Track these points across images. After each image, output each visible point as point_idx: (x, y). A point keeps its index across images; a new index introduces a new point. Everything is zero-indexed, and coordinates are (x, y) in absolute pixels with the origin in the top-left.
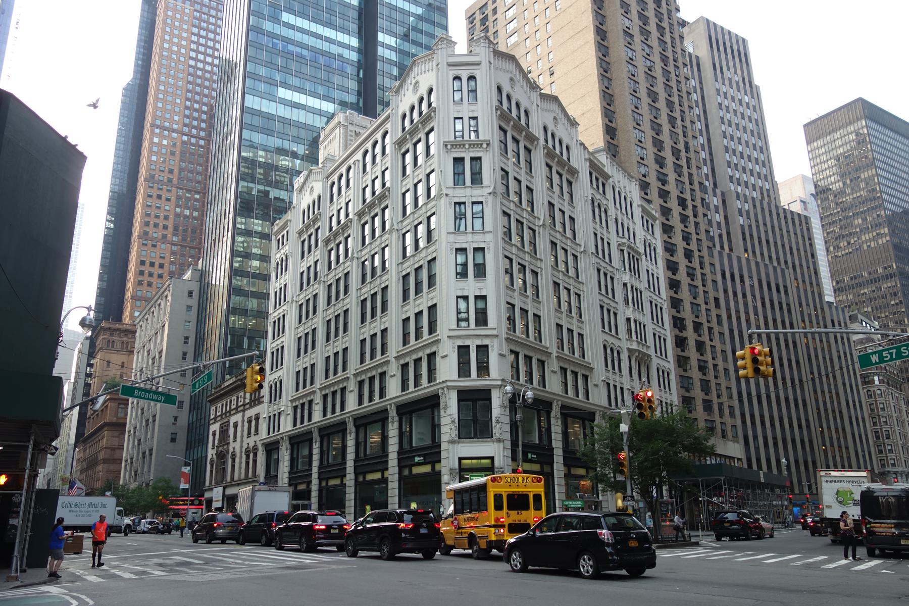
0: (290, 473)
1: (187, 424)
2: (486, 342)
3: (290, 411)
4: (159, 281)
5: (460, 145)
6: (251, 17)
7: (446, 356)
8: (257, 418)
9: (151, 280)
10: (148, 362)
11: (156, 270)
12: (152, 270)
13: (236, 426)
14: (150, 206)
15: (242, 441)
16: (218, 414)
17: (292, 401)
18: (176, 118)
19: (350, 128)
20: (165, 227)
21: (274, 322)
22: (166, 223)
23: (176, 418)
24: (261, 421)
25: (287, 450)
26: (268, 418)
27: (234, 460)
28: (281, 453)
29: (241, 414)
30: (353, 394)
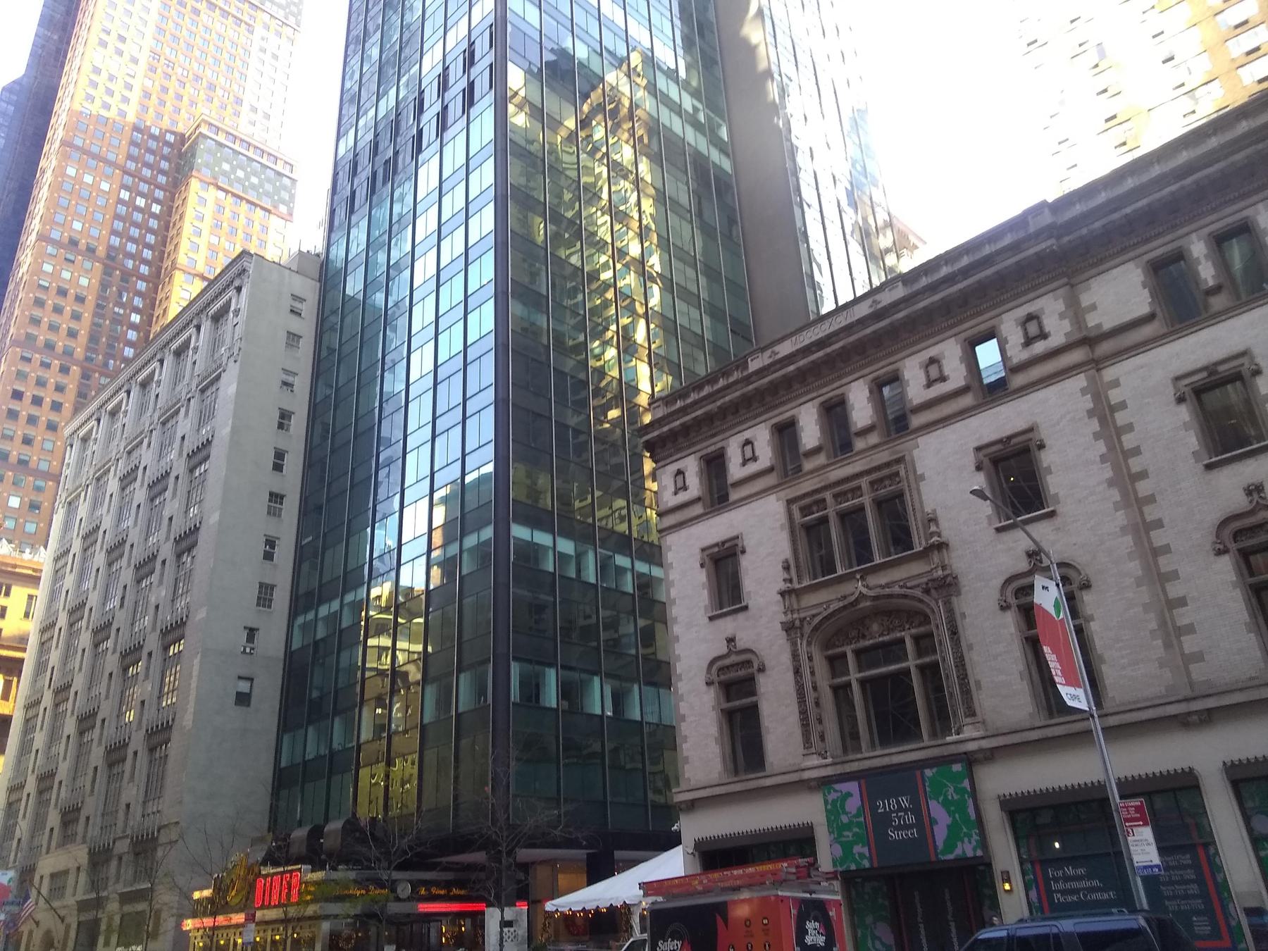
1: (281, 654)
4: (49, 435)
9: (31, 431)
11: (45, 414)
12: (34, 411)
20: (72, 334)
22: (74, 325)
23: (252, 633)
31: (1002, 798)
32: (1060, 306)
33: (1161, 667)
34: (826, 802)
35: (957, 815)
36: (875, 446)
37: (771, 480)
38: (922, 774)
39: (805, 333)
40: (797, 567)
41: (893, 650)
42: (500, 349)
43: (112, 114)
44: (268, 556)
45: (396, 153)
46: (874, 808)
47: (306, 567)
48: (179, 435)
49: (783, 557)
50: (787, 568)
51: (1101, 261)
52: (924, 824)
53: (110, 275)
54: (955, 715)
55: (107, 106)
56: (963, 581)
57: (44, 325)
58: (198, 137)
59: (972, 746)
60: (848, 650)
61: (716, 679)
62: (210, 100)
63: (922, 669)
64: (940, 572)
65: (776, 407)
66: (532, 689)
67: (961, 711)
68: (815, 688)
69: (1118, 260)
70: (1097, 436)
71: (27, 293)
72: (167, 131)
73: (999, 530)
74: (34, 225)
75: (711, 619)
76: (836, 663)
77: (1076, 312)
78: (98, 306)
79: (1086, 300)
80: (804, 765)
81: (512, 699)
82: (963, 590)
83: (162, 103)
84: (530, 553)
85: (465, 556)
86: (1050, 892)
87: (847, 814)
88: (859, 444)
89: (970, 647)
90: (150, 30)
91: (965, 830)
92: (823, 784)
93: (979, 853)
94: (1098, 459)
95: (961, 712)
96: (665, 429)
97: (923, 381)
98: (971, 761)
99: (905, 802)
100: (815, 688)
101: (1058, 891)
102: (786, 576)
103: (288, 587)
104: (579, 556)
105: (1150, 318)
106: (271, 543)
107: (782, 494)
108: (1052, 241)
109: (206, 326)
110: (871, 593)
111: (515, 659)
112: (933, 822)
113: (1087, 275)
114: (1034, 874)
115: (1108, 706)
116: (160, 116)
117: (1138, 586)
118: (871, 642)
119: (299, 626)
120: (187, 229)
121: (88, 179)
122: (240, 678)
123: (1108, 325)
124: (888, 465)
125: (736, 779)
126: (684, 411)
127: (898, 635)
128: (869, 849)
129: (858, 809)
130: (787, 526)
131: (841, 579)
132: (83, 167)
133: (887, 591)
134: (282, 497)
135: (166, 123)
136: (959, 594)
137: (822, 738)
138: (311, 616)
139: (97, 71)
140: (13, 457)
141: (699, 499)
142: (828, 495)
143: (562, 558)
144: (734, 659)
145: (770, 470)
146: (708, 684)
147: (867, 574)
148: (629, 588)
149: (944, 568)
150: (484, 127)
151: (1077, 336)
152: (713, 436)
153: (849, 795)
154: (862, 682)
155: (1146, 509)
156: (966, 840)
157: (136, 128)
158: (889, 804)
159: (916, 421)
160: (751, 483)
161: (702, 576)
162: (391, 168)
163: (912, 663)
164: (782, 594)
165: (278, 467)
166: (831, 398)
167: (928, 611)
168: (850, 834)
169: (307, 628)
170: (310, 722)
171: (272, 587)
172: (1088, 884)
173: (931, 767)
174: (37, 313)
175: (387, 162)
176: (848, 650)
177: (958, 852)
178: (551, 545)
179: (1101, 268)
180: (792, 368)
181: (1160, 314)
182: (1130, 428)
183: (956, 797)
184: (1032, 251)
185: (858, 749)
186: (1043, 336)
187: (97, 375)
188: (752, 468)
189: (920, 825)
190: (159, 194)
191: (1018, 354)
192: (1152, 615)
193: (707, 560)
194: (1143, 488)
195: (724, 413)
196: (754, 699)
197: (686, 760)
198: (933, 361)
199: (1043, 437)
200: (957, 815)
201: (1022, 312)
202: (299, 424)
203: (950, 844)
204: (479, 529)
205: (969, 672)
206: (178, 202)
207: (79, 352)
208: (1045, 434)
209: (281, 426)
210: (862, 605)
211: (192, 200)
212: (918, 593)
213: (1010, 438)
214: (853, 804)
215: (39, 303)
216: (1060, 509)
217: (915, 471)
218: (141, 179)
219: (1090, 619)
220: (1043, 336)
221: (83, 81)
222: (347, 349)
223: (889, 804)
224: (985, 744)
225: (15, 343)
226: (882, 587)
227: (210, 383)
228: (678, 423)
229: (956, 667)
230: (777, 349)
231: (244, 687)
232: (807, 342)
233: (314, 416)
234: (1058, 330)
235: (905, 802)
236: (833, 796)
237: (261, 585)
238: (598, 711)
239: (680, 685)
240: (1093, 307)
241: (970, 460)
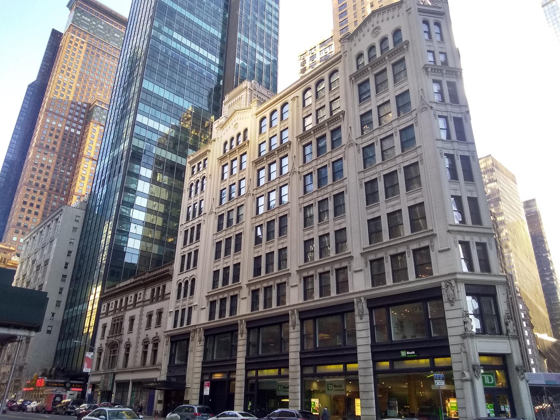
0: (203, 363)
2: (484, 240)
3: (205, 304)
4: (35, 217)
5: (438, 70)
6: (153, 30)
7: (448, 250)
8: (160, 313)
9: (29, 216)
10: (32, 270)
11: (34, 209)
12: (30, 208)
13: (132, 320)
14: (37, 164)
15: (139, 333)
16: (110, 309)
17: (208, 297)
18: (64, 109)
19: (254, 92)
20: (45, 180)
21: (186, 232)
23: (53, 314)
24: (163, 315)
25: (200, 341)
26: (174, 312)
27: (128, 349)
28: (191, 344)
29: (140, 309)
30: (296, 289)
43: (64, 98)
44: (60, 293)
53: (60, 158)
55: (62, 95)
58: (94, 107)
59: (115, 371)
62: (101, 90)
71: (30, 166)
72: (84, 103)
74: (35, 140)
78: (55, 170)
83: (83, 92)
120: (88, 141)
121: (54, 123)
122: (49, 326)
132: (52, 119)
139: (59, 82)
140: (23, 224)
157: (73, 103)
165: (66, 267)
171: (61, 301)
174: (33, 173)
187: (53, 195)
190: (80, 127)
202: (74, 255)
206: (86, 130)
207: (47, 187)
209: (68, 255)
211: (91, 130)
215: (34, 170)
221: (55, 86)
225: (25, 185)
231: (50, 329)
237: (57, 301)
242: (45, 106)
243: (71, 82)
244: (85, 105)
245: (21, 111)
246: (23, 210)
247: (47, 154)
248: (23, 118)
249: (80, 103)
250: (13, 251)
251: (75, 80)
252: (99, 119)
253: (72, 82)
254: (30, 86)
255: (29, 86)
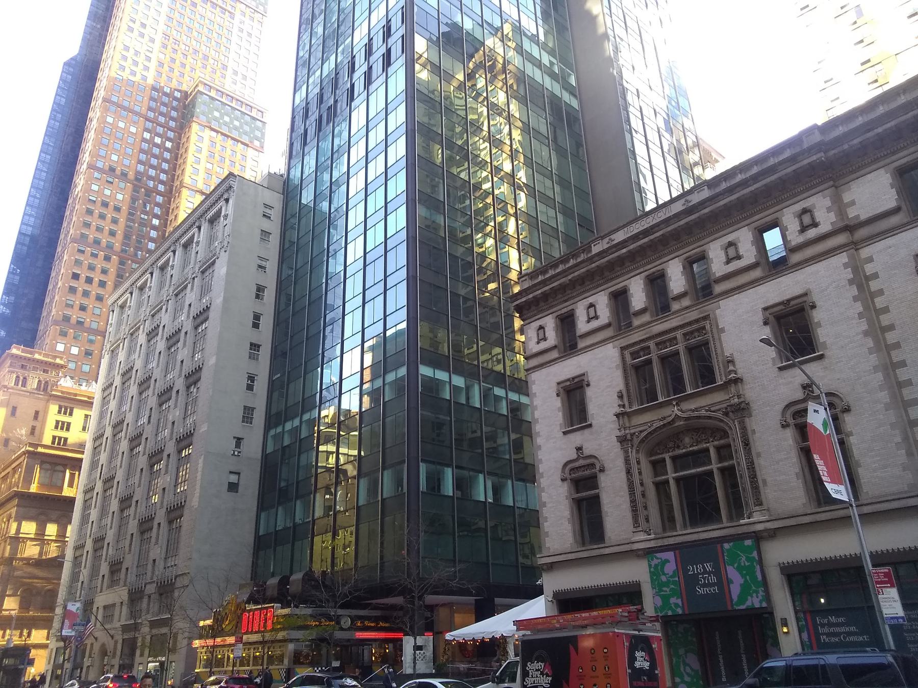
4: (98, 304)
11: (94, 290)
12: (87, 287)
22: (114, 227)
23: (239, 441)
31: (782, 565)
32: (827, 202)
33: (904, 470)
34: (650, 566)
35: (748, 577)
36: (687, 308)
37: (609, 333)
38: (722, 547)
39: (634, 225)
40: (629, 396)
41: (701, 456)
42: (410, 240)
43: (137, 78)
44: (250, 388)
45: (336, 102)
46: (686, 571)
47: (276, 395)
48: (187, 303)
49: (618, 389)
50: (621, 397)
51: (860, 168)
52: (723, 583)
54: (747, 504)
55: (133, 73)
56: (754, 407)
57: (93, 228)
58: (196, 93)
59: (760, 527)
60: (667, 456)
61: (568, 477)
62: (205, 67)
63: (722, 470)
64: (736, 400)
65: (612, 279)
66: (435, 482)
67: (751, 502)
68: (642, 484)
69: (874, 167)
70: (855, 299)
72: (175, 90)
73: (780, 369)
74: (85, 158)
75: (565, 433)
76: (658, 466)
77: (839, 207)
78: (130, 214)
79: (847, 197)
80: (633, 539)
81: (421, 489)
82: (754, 413)
83: (172, 70)
84: (433, 386)
85: (387, 387)
86: (818, 635)
87: (664, 574)
88: (675, 306)
89: (759, 455)
90: (163, 19)
91: (754, 588)
92: (648, 553)
93: (764, 605)
94: (857, 316)
95: (751, 502)
96: (531, 296)
97: (724, 259)
98: (758, 538)
99: (709, 567)
100: (642, 484)
101: (825, 634)
102: (621, 403)
103: (264, 409)
104: (468, 388)
105: (896, 211)
106: (251, 378)
107: (617, 343)
108: (822, 154)
109: (205, 227)
110: (684, 415)
111: (423, 461)
112: (729, 582)
113: (848, 179)
114: (806, 620)
115: (863, 499)
116: (170, 79)
117: (887, 410)
118: (684, 451)
119: (272, 436)
120: (190, 159)
121: (121, 125)
123: (863, 217)
124: (697, 321)
125: (583, 549)
126: (544, 283)
127: (705, 446)
128: (682, 601)
129: (674, 572)
130: (621, 367)
131: (661, 405)
133: (696, 414)
134: (259, 346)
135: (174, 84)
136: (750, 416)
137: (647, 520)
138: (279, 429)
139: (127, 48)
141: (555, 347)
142: (652, 344)
143: (456, 389)
144: (582, 462)
145: (608, 325)
146: (563, 480)
147: (681, 401)
148: (504, 411)
149: (739, 397)
150: (398, 81)
151: (841, 224)
152: (566, 301)
153: (667, 561)
154: (678, 480)
155: (894, 353)
156: (754, 595)
157: (154, 88)
158: (697, 568)
159: (718, 289)
160: (594, 335)
161: (558, 403)
162: (332, 113)
163: (714, 466)
164: (617, 415)
165: (256, 326)
166: (654, 273)
167: (727, 428)
168: (668, 590)
169: (279, 437)
170: (279, 504)
171: (253, 409)
172: (847, 629)
173: (728, 542)
174: (88, 219)
175: (330, 108)
176: (667, 456)
177: (749, 603)
178: (448, 381)
179: (858, 174)
180: (624, 251)
181: (904, 207)
182: (881, 292)
183: (747, 564)
184: (806, 162)
185: (674, 528)
186: (815, 225)
187: (130, 262)
188: (595, 324)
189: (719, 583)
190: (171, 134)
191: (796, 239)
192: (897, 432)
193: (562, 391)
194: (891, 337)
195: (573, 284)
196: (597, 491)
197: (547, 534)
198: (731, 244)
199: (814, 299)
200: (748, 577)
201: (798, 207)
202: (270, 295)
203: (742, 598)
204: (396, 369)
205: (758, 473)
207: (117, 246)
208: (816, 297)
209: (257, 297)
210: (677, 424)
211: (193, 138)
212: (719, 415)
213: (789, 301)
214: (670, 568)
215: (90, 212)
216: (828, 353)
217: (717, 326)
218: (158, 125)
219: (850, 434)
220: (815, 225)
221: (117, 57)
222: (302, 242)
223: (697, 568)
224: (770, 525)
225: (74, 241)
226: (693, 411)
227: (208, 266)
228: (540, 292)
229: (748, 469)
230: (612, 237)
231: (233, 478)
232: (636, 231)
233: (280, 289)
234: (826, 220)
235: (709, 567)
236: (655, 561)
237: (245, 407)
238: (482, 499)
239: (542, 480)
240: (853, 203)
241: (759, 317)
242: (102, 93)
243: (148, 50)
244: (177, 94)
245: (53, 110)
246: (73, 290)
247: (112, 183)
248: (58, 124)
249: (167, 90)
250: (62, 367)
251: (157, 46)
252: (207, 117)
253: (151, 50)
254: (67, 64)
255: (65, 64)
